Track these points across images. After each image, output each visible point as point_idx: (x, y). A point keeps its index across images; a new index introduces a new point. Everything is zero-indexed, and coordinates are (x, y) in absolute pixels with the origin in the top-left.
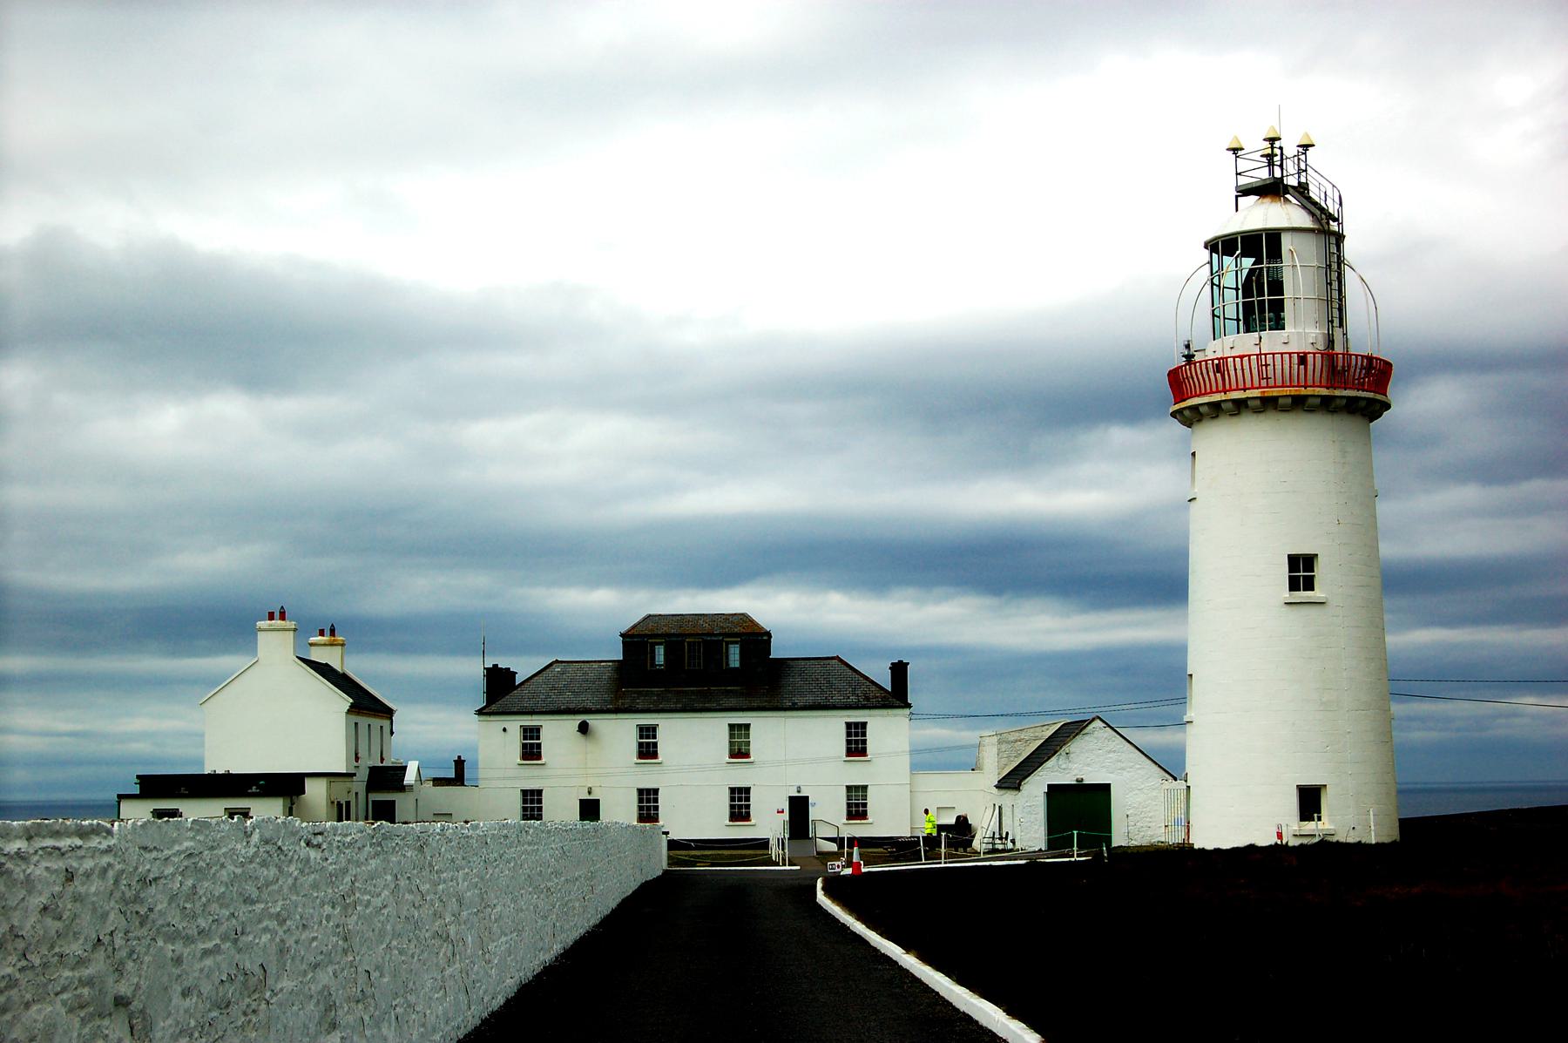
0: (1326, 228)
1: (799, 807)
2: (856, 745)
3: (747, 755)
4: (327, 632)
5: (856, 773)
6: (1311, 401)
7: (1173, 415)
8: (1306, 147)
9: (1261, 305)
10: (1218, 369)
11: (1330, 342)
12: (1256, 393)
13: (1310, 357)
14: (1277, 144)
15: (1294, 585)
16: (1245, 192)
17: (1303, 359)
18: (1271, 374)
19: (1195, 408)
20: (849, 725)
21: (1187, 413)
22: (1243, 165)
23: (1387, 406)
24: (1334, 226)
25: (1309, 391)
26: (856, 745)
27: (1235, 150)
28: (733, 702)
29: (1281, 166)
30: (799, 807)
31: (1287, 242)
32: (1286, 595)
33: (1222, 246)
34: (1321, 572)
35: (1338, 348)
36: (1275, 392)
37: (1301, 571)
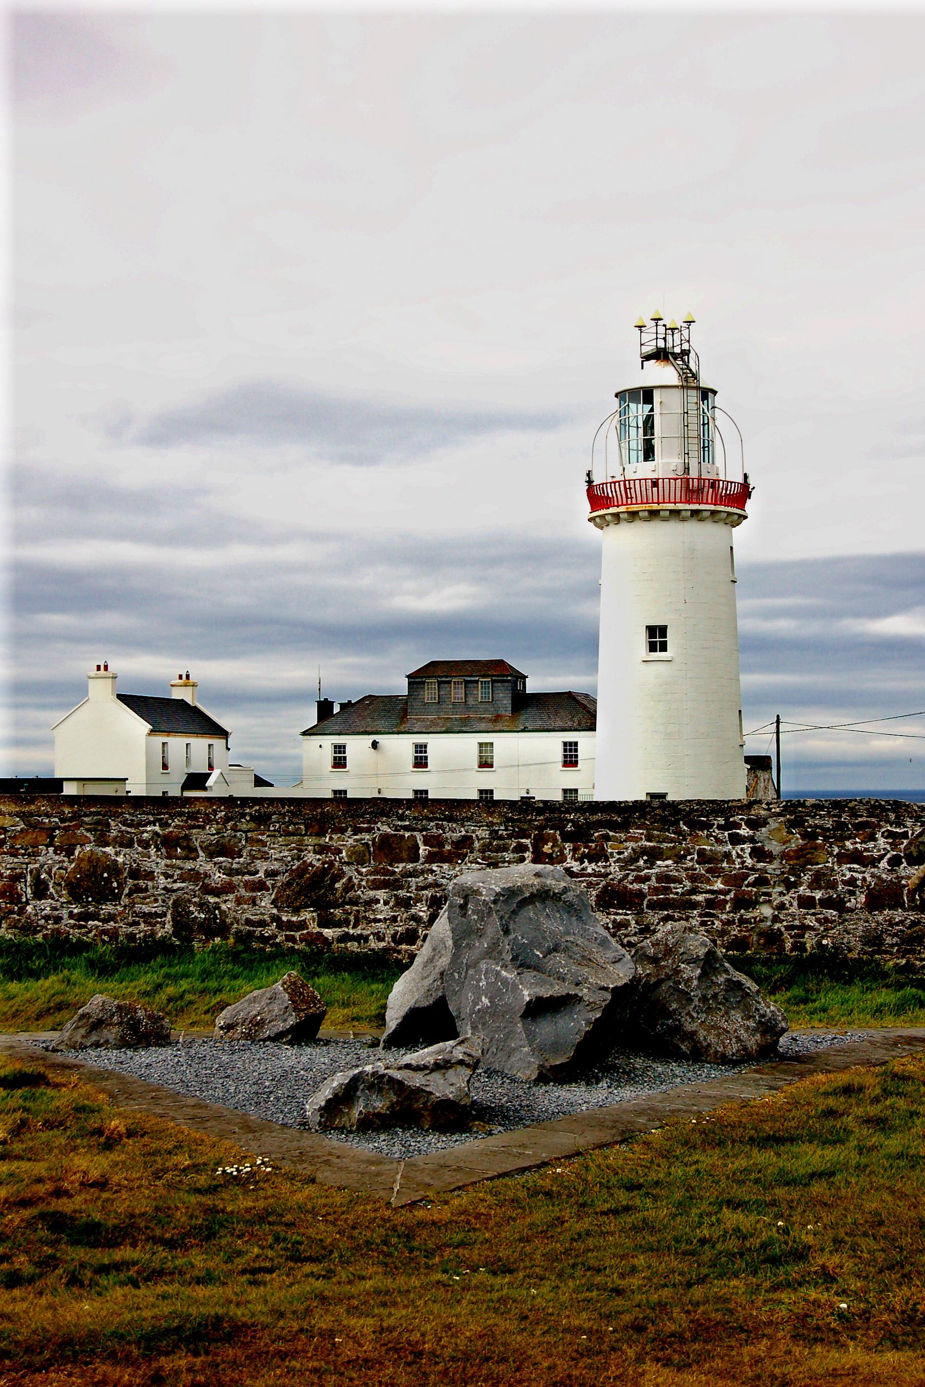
3: (491, 766)
4: (184, 677)
6: (683, 513)
7: (590, 520)
11: (687, 469)
13: (660, 481)
14: (660, 323)
15: (652, 648)
16: (648, 358)
17: (655, 483)
18: (634, 495)
19: (602, 517)
20: (565, 744)
21: (598, 520)
26: (570, 758)
28: (483, 726)
29: (665, 339)
31: (657, 396)
34: (669, 639)
37: (657, 637)
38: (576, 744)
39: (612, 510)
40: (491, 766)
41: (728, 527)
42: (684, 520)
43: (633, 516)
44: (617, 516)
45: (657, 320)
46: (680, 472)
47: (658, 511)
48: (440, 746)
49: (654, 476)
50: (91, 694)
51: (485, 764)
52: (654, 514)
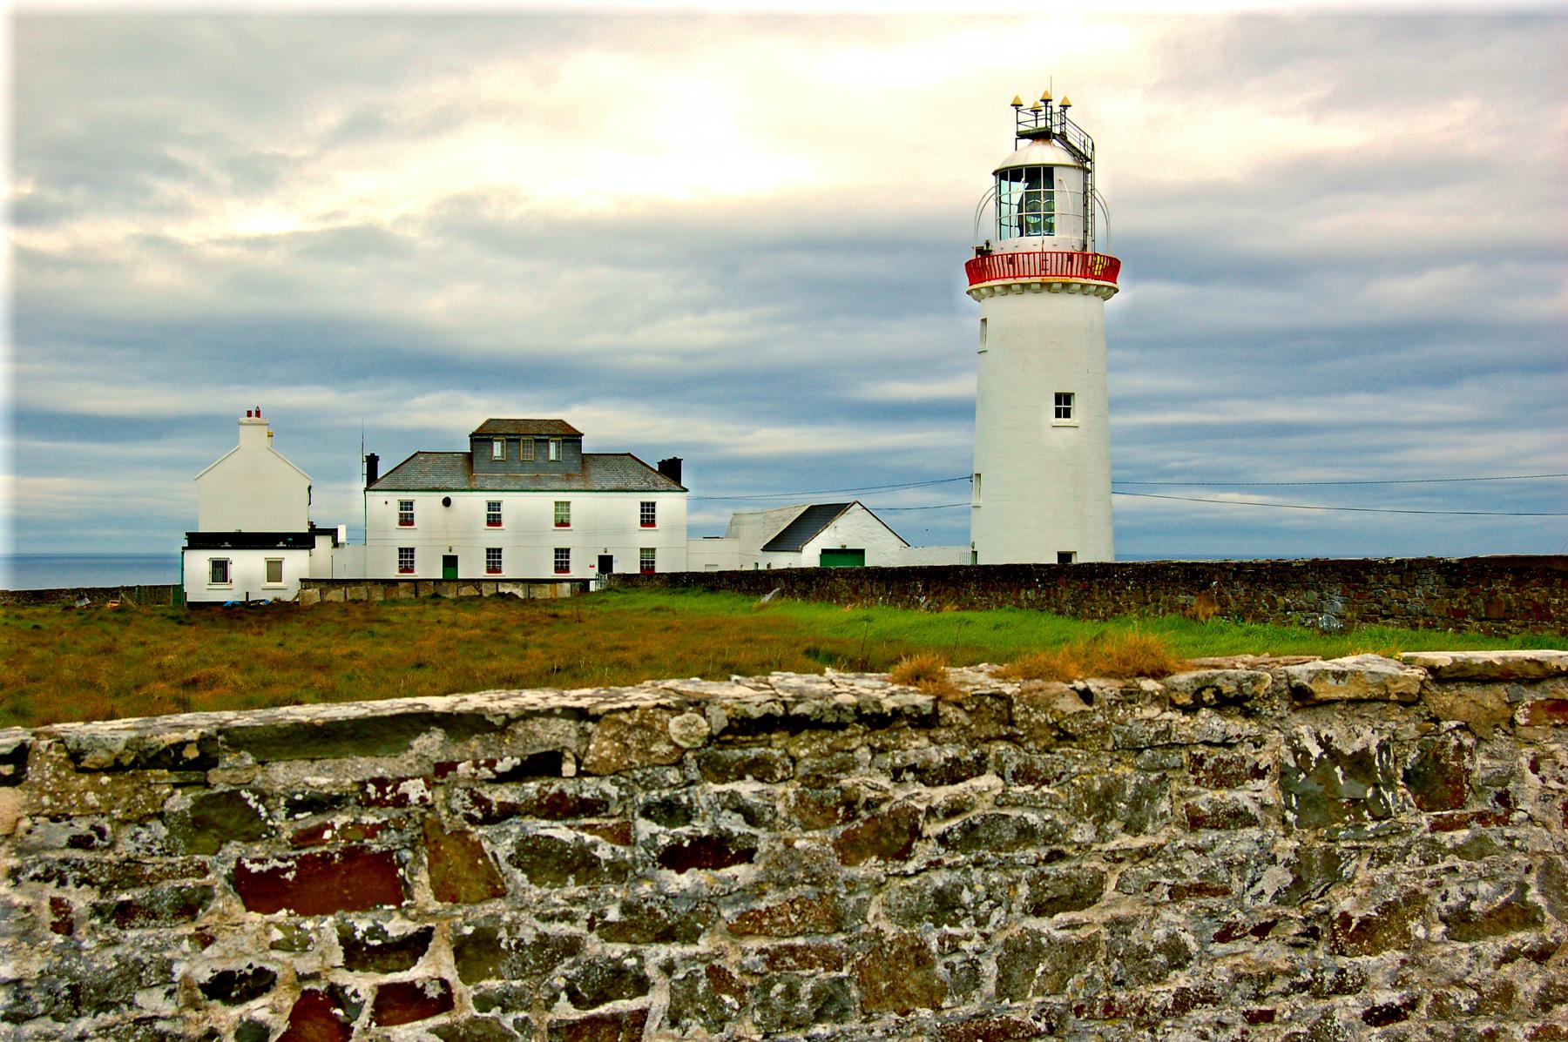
0: (1083, 161)
1: (450, 562)
2: (648, 517)
3: (568, 525)
5: (647, 538)
8: (1065, 107)
9: (1034, 218)
10: (1011, 261)
11: (1085, 246)
12: (1038, 279)
15: (1058, 415)
17: (1071, 257)
22: (1022, 117)
23: (1116, 291)
24: (1088, 165)
26: (648, 517)
27: (1017, 106)
28: (557, 485)
30: (450, 562)
31: (1058, 174)
33: (1008, 174)
34: (1077, 406)
35: (1089, 251)
36: (1050, 279)
37: (1063, 403)
38: (653, 504)
39: (987, 284)
40: (568, 525)
41: (1099, 299)
42: (1056, 292)
43: (1046, 286)
44: (1008, 287)
45: (1046, 101)
46: (1078, 248)
47: (1050, 284)
48: (514, 504)
49: (1070, 250)
50: (242, 442)
51: (562, 523)
52: (1066, 286)
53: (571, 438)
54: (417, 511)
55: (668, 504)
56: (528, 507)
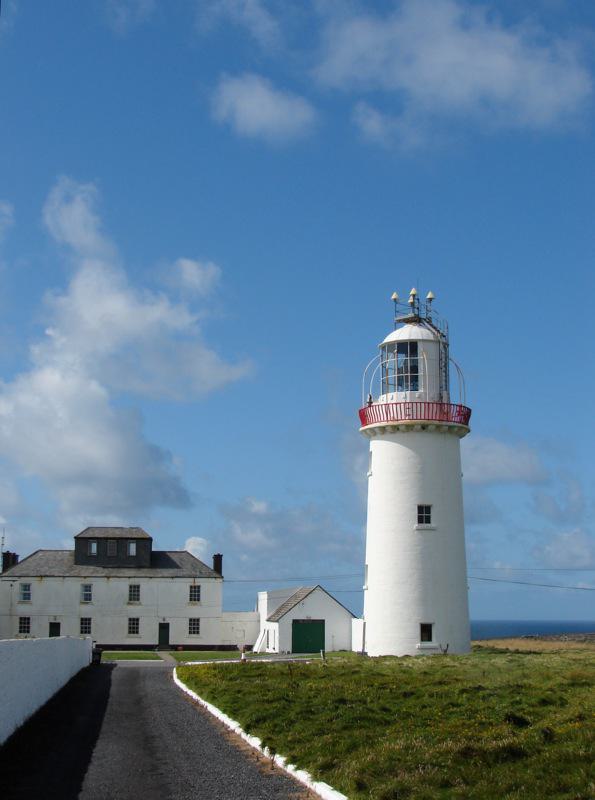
1: (164, 628)
6: (430, 427)
11: (441, 398)
15: (420, 520)
19: (372, 429)
25: (429, 422)
26: (195, 594)
30: (164, 628)
31: (420, 345)
32: (416, 525)
34: (433, 514)
35: (445, 401)
46: (436, 400)
53: (145, 542)
54: (94, 591)
55: (207, 586)
56: (111, 588)
